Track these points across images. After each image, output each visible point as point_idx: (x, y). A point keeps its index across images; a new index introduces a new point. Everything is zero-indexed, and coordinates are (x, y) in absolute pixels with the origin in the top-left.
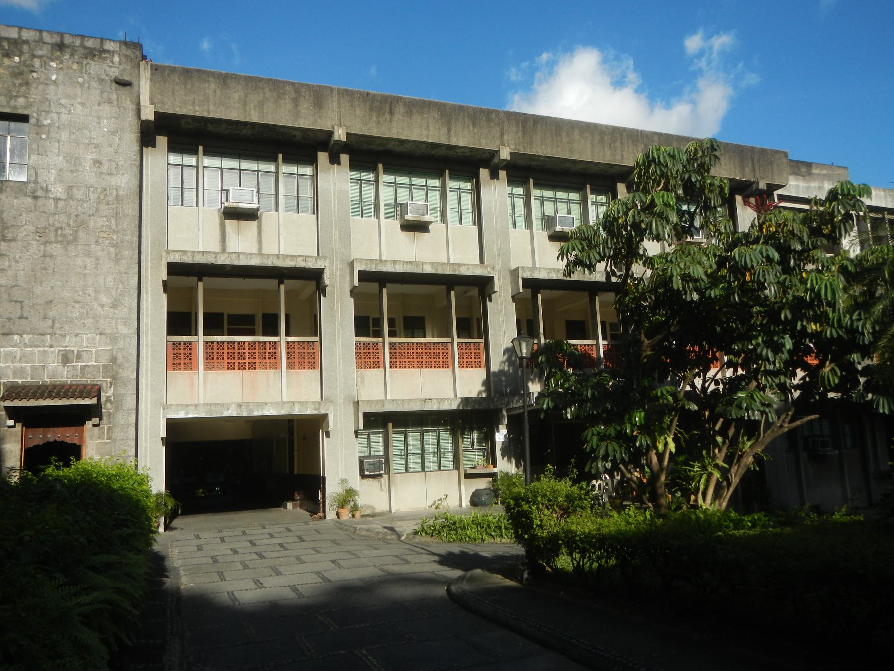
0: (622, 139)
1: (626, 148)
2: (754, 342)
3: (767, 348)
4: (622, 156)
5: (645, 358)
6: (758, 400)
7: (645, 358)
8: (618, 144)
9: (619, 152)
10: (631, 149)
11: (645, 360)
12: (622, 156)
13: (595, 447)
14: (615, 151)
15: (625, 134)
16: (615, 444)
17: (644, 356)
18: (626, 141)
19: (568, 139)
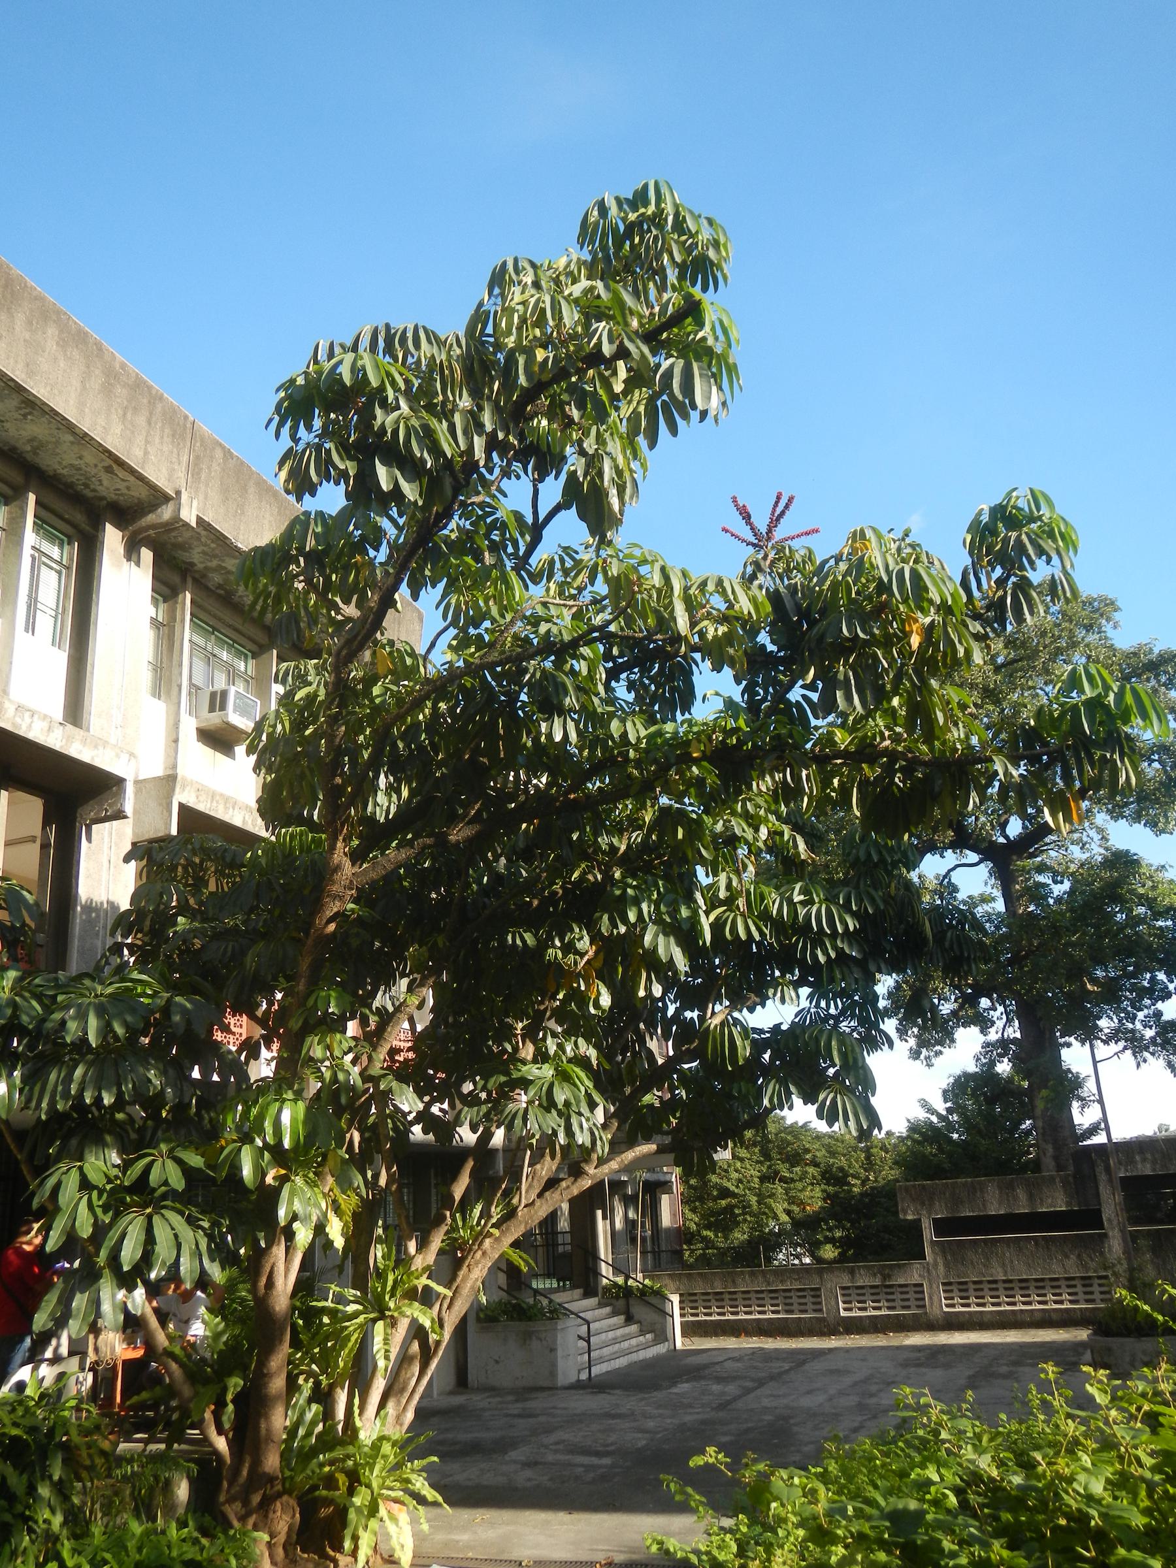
0: (151, 414)
1: (157, 440)
2: (632, 916)
3: (666, 935)
4: (146, 453)
5: (330, 921)
6: (582, 1089)
7: (330, 921)
8: (141, 420)
9: (140, 439)
10: (165, 449)
11: (332, 927)
12: (146, 453)
13: (85, 1231)
14: (133, 432)
15: (159, 406)
16: (176, 1220)
17: (329, 914)
18: (159, 424)
19: (27, 335)
